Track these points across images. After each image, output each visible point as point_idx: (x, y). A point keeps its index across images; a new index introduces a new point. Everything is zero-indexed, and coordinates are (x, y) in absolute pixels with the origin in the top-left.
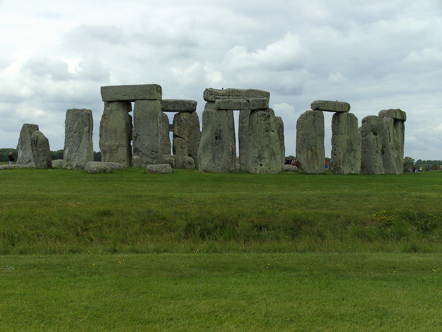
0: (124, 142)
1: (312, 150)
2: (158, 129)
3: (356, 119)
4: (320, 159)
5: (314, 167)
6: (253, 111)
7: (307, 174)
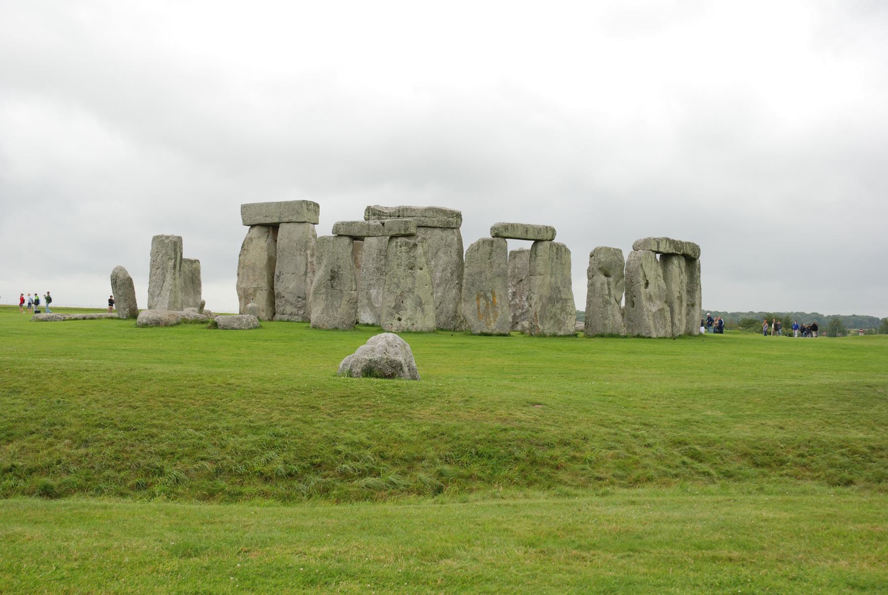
0: (264, 284)
1: (486, 298)
2: (307, 265)
3: (567, 251)
4: (500, 312)
5: (488, 324)
6: (392, 237)
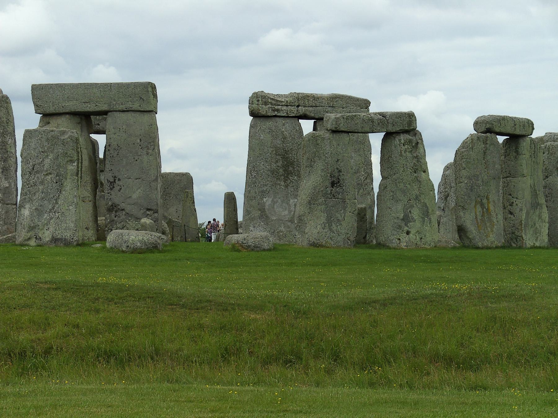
1: (482, 205)
4: (495, 220)
5: (487, 236)
7: (478, 248)
